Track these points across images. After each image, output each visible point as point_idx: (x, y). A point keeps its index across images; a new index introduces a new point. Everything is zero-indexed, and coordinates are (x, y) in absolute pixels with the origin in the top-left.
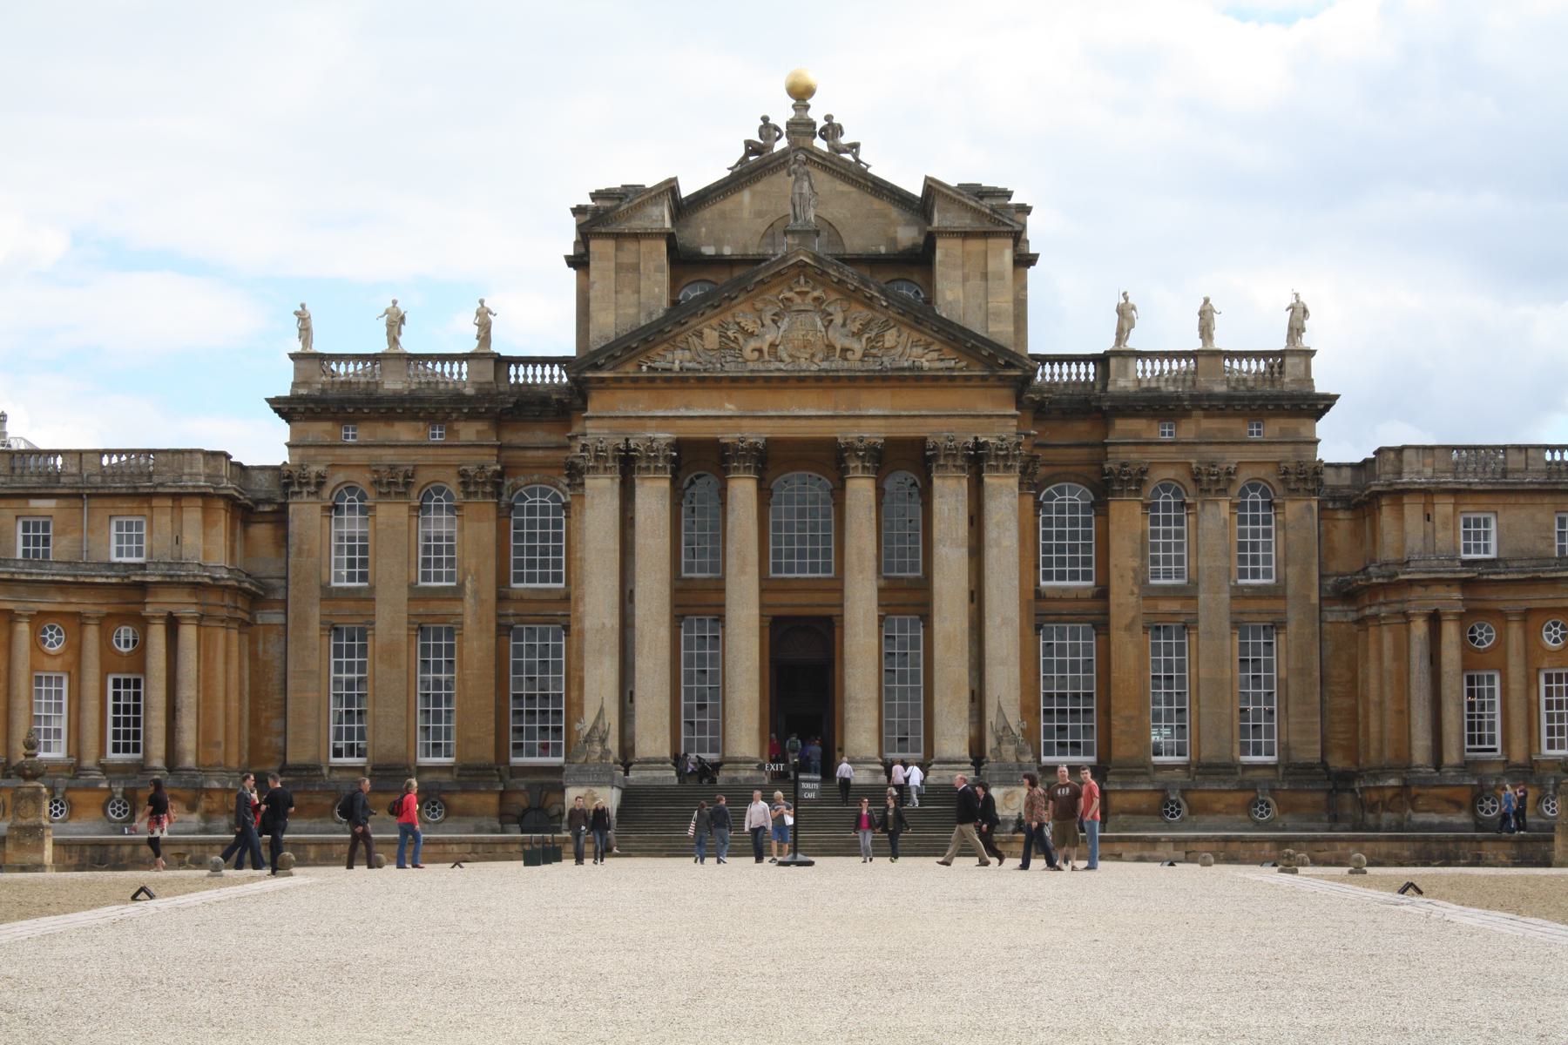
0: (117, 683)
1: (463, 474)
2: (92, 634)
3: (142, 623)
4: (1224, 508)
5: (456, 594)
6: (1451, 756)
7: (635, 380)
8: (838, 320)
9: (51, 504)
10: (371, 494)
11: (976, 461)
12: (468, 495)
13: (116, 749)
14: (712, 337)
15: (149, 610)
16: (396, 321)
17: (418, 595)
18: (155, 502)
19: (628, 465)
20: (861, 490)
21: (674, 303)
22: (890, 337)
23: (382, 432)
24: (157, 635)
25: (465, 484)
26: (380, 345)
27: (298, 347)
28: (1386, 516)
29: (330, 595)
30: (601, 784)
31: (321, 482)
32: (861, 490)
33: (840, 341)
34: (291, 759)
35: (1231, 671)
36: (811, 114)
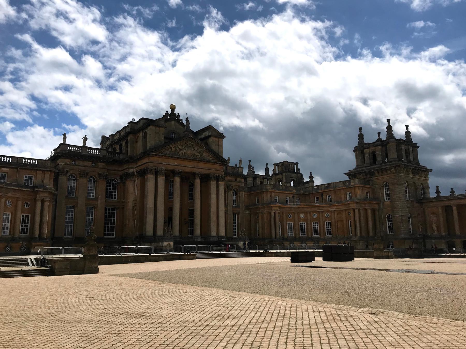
0: (23, 216)
1: (99, 174)
2: (20, 202)
3: (35, 201)
4: (232, 192)
5: (96, 199)
6: (278, 237)
7: (159, 155)
8: (196, 149)
9: (8, 169)
10: (78, 176)
11: (218, 179)
12: (100, 178)
13: (21, 233)
14: (173, 149)
15: (38, 198)
16: (85, 139)
17: (88, 199)
18: (38, 172)
19: (157, 173)
20: (198, 183)
21: (165, 143)
22: (204, 154)
23: (81, 163)
24: (39, 204)
25: (99, 176)
26: (81, 144)
27: (62, 142)
28: (264, 194)
29: (67, 198)
30: (171, 241)
31: (67, 172)
32: (198, 183)
33: (196, 154)
34: (55, 236)
35: (233, 221)
36: (175, 112)
